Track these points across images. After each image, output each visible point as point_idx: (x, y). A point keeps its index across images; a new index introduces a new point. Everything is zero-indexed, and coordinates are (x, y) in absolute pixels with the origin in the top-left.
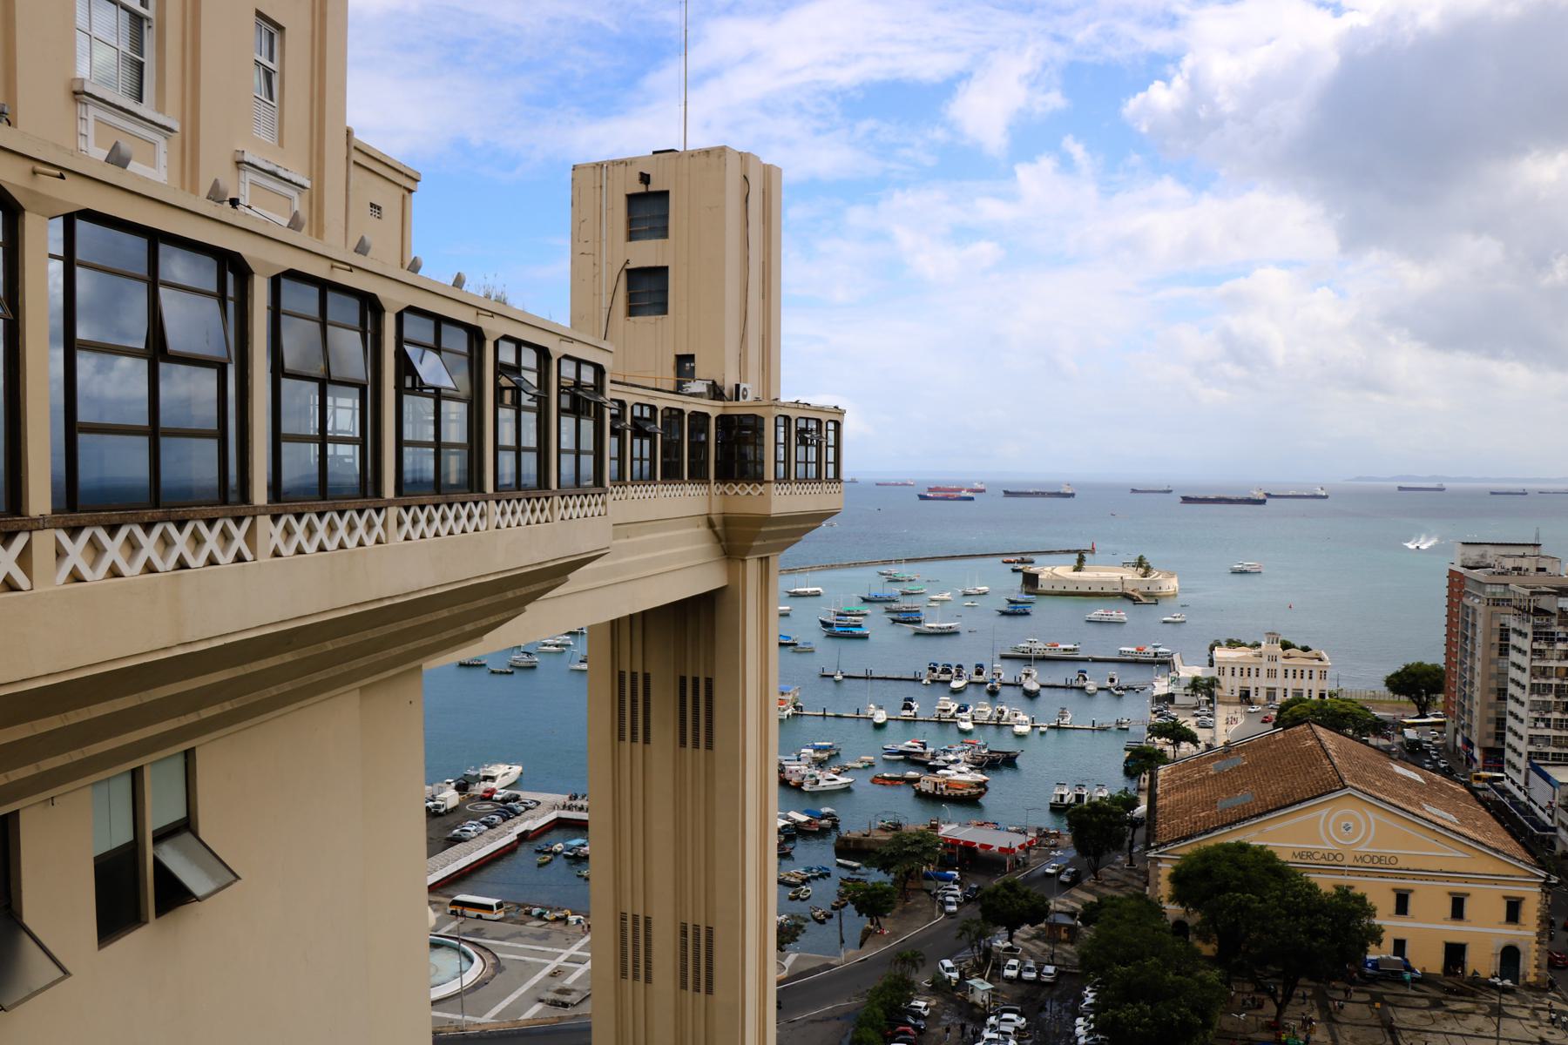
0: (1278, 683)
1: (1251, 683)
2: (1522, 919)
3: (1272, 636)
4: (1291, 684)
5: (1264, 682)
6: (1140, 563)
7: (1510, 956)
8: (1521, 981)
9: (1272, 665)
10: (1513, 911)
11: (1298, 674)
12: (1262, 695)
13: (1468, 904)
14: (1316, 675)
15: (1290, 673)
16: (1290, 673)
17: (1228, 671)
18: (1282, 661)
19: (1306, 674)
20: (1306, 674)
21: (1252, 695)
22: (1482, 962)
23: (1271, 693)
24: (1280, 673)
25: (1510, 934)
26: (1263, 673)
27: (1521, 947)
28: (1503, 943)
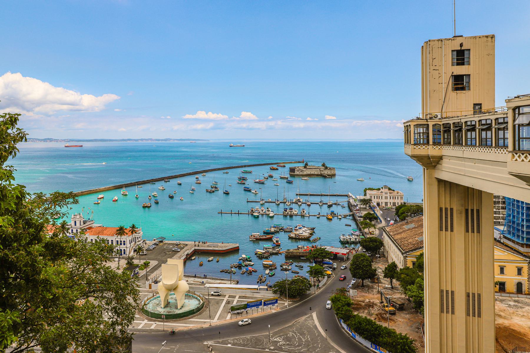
0: (388, 200)
1: (380, 201)
2: (522, 274)
3: (386, 187)
4: (392, 201)
5: (384, 201)
6: (324, 165)
7: (519, 285)
8: (523, 293)
9: (386, 195)
10: (519, 271)
11: (394, 198)
12: (384, 205)
13: (505, 269)
14: (399, 198)
15: (392, 198)
16: (392, 198)
17: (373, 197)
18: (388, 194)
19: (397, 198)
20: (397, 198)
21: (381, 204)
22: (511, 287)
23: (386, 204)
24: (389, 198)
25: (519, 279)
26: (384, 198)
27: (523, 282)
28: (517, 281)
